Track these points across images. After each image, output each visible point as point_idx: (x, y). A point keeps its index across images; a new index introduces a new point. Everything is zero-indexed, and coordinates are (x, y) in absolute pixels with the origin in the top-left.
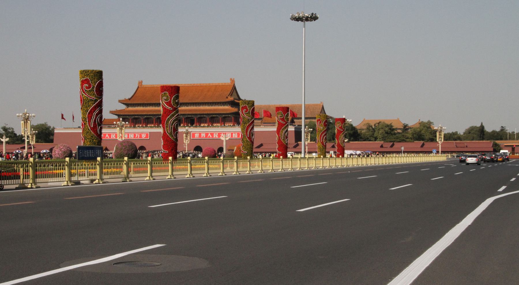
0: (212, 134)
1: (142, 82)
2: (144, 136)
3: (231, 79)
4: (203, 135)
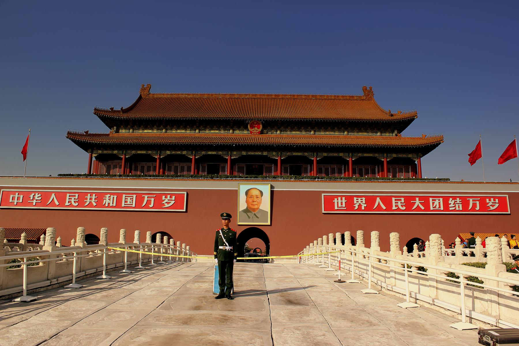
0: (387, 201)
2: (168, 202)
3: (365, 89)
4: (360, 202)
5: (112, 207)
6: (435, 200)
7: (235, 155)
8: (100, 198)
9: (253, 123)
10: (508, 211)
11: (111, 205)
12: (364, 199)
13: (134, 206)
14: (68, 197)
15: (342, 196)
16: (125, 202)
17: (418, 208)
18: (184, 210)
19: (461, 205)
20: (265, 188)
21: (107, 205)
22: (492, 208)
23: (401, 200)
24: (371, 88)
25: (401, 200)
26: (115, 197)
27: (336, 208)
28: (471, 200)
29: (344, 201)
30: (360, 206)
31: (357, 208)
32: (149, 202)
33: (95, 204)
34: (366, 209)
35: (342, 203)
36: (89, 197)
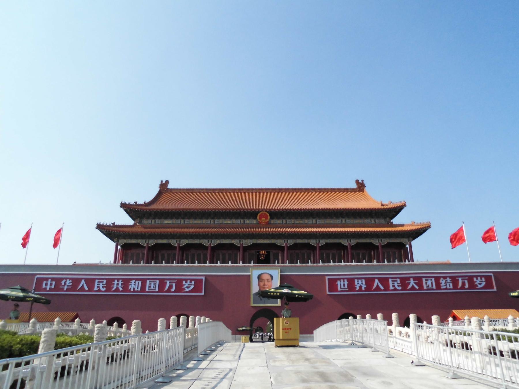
1: (167, 182)
2: (188, 287)
3: (357, 182)
5: (138, 292)
6: (427, 280)
7: (248, 242)
8: (126, 282)
9: (262, 214)
10: (493, 288)
11: (136, 289)
12: (364, 280)
13: (157, 290)
14: (96, 283)
15: (344, 279)
16: (150, 287)
17: (413, 288)
18: (203, 294)
19: (451, 284)
20: (276, 273)
21: (132, 290)
22: (480, 286)
23: (397, 281)
24: (363, 181)
25: (397, 281)
26: (140, 282)
27: (339, 289)
28: (460, 279)
29: (346, 283)
30: (361, 287)
31: (358, 288)
32: (171, 287)
33: (121, 289)
34: (366, 290)
35: (344, 285)
36: (116, 282)
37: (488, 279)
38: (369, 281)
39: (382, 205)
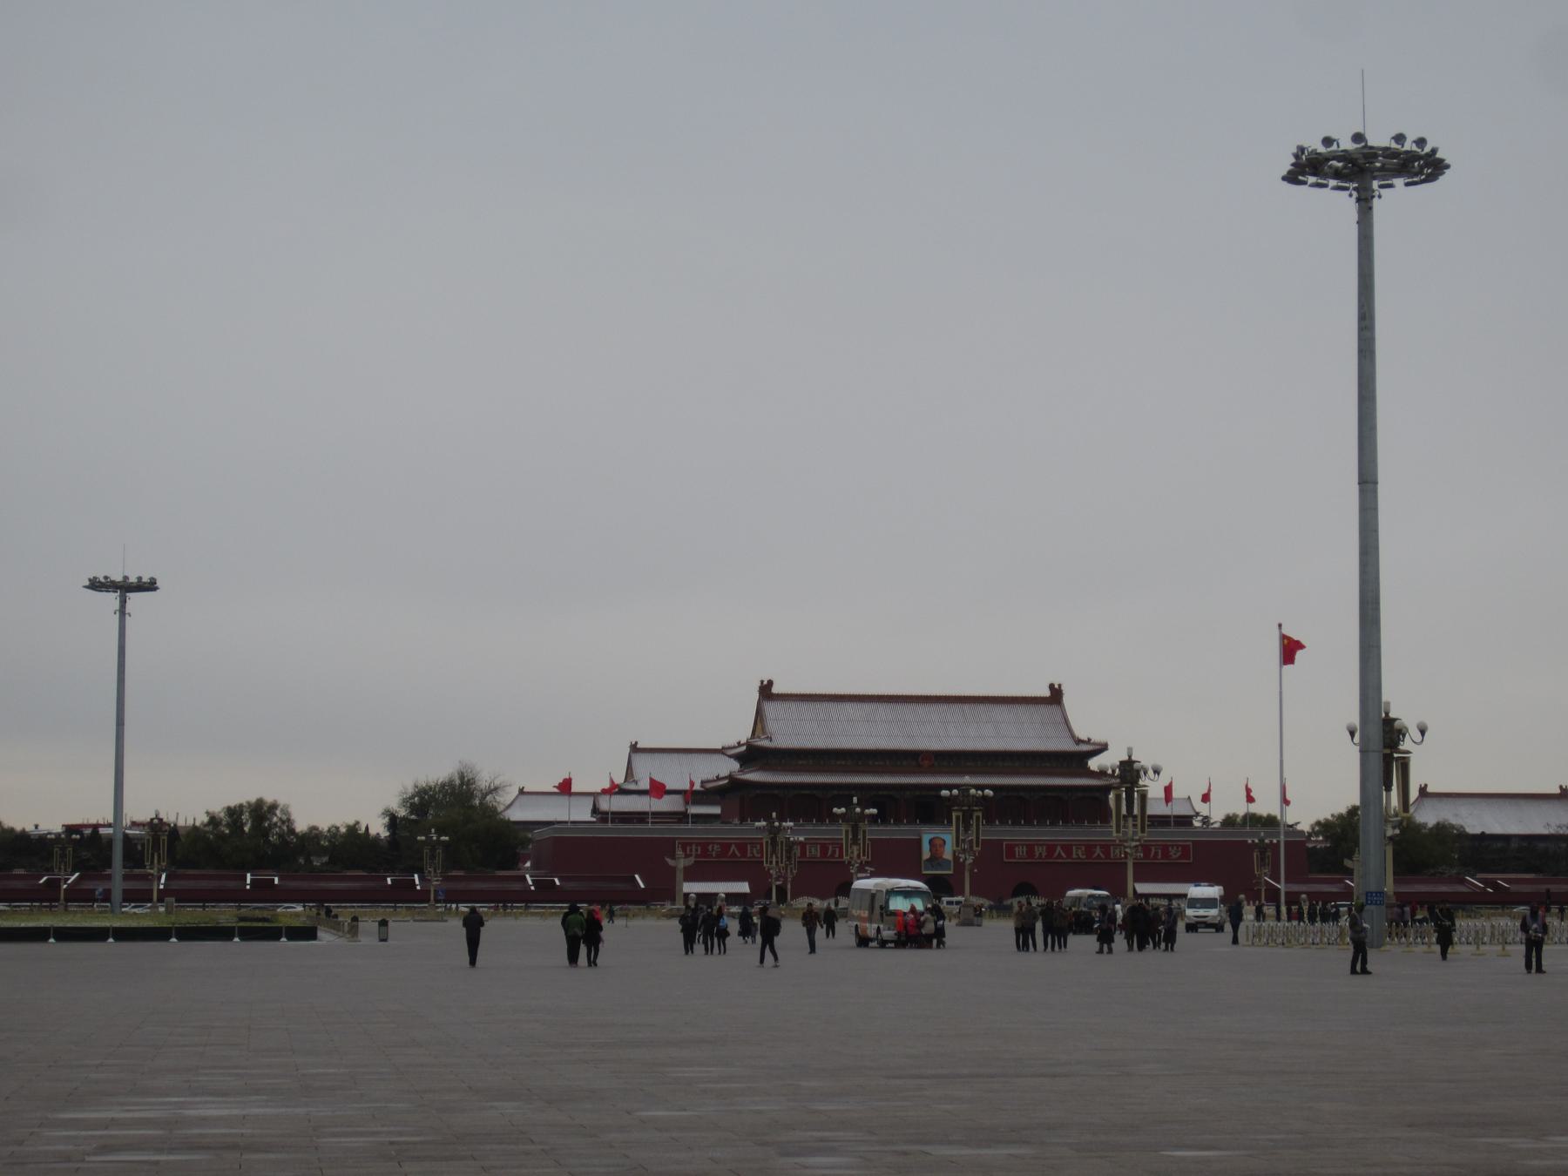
1: (770, 683)
3: (1051, 686)
37: (1185, 849)
38: (1051, 848)
39: (1079, 741)
